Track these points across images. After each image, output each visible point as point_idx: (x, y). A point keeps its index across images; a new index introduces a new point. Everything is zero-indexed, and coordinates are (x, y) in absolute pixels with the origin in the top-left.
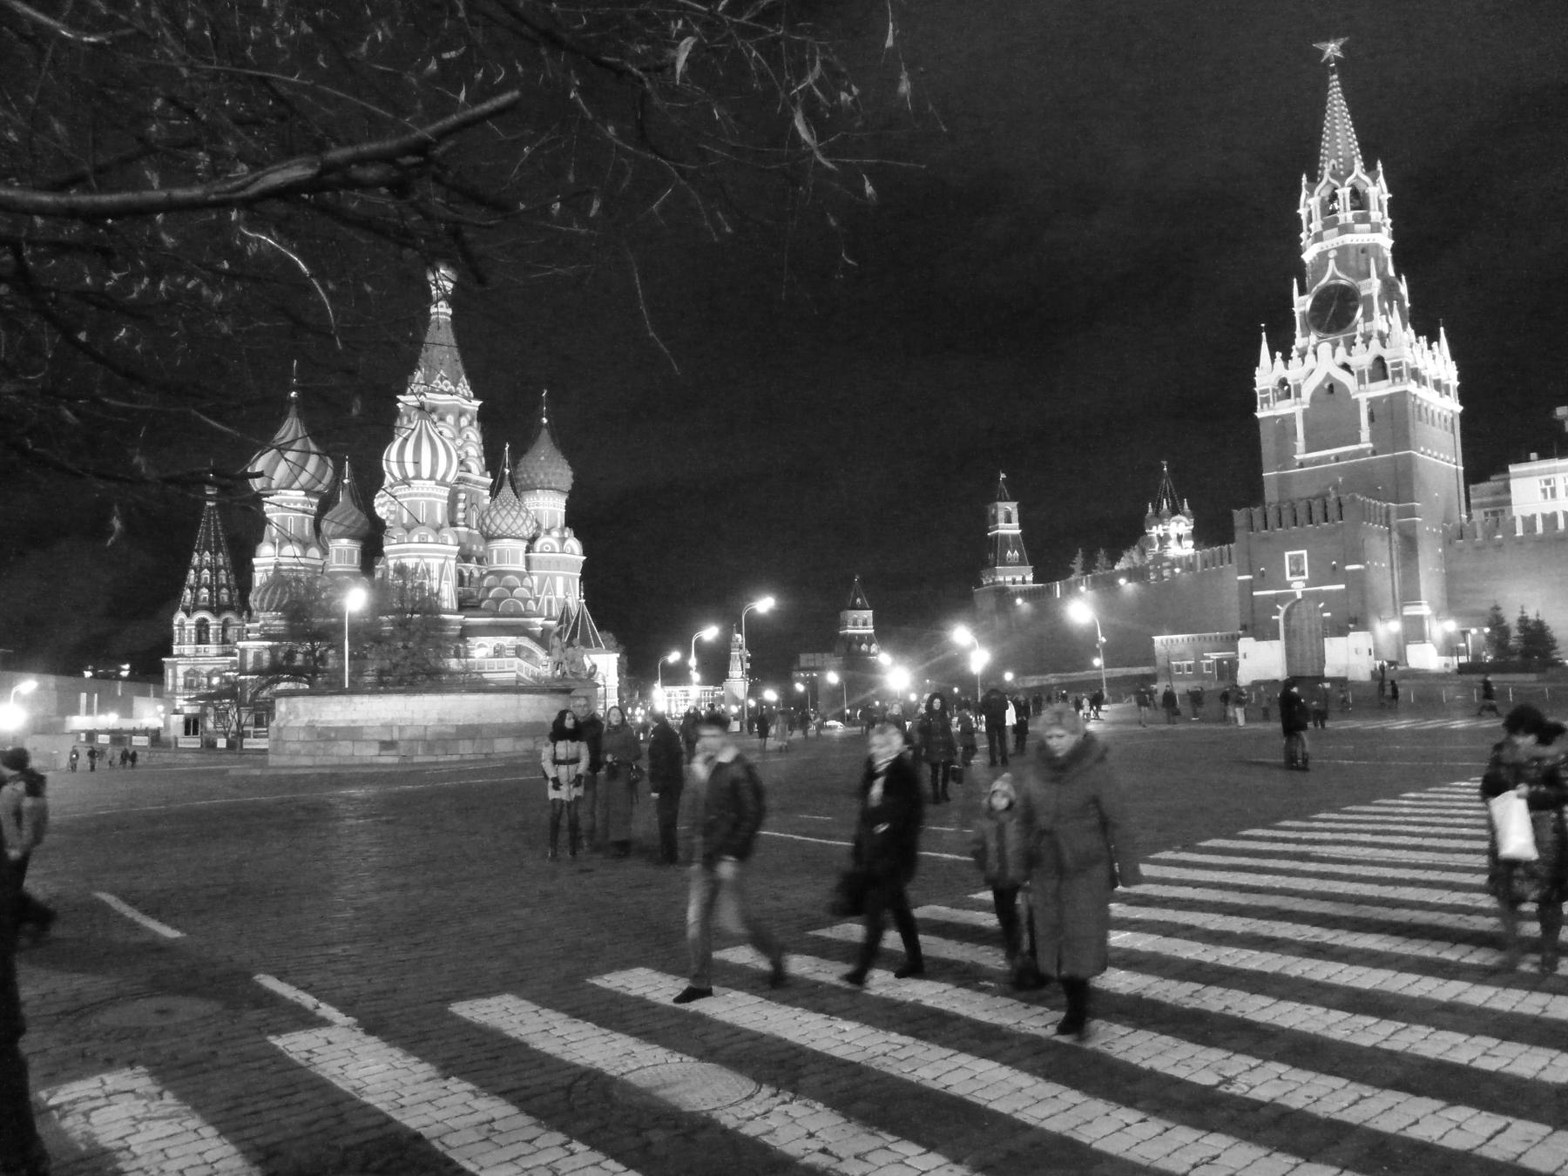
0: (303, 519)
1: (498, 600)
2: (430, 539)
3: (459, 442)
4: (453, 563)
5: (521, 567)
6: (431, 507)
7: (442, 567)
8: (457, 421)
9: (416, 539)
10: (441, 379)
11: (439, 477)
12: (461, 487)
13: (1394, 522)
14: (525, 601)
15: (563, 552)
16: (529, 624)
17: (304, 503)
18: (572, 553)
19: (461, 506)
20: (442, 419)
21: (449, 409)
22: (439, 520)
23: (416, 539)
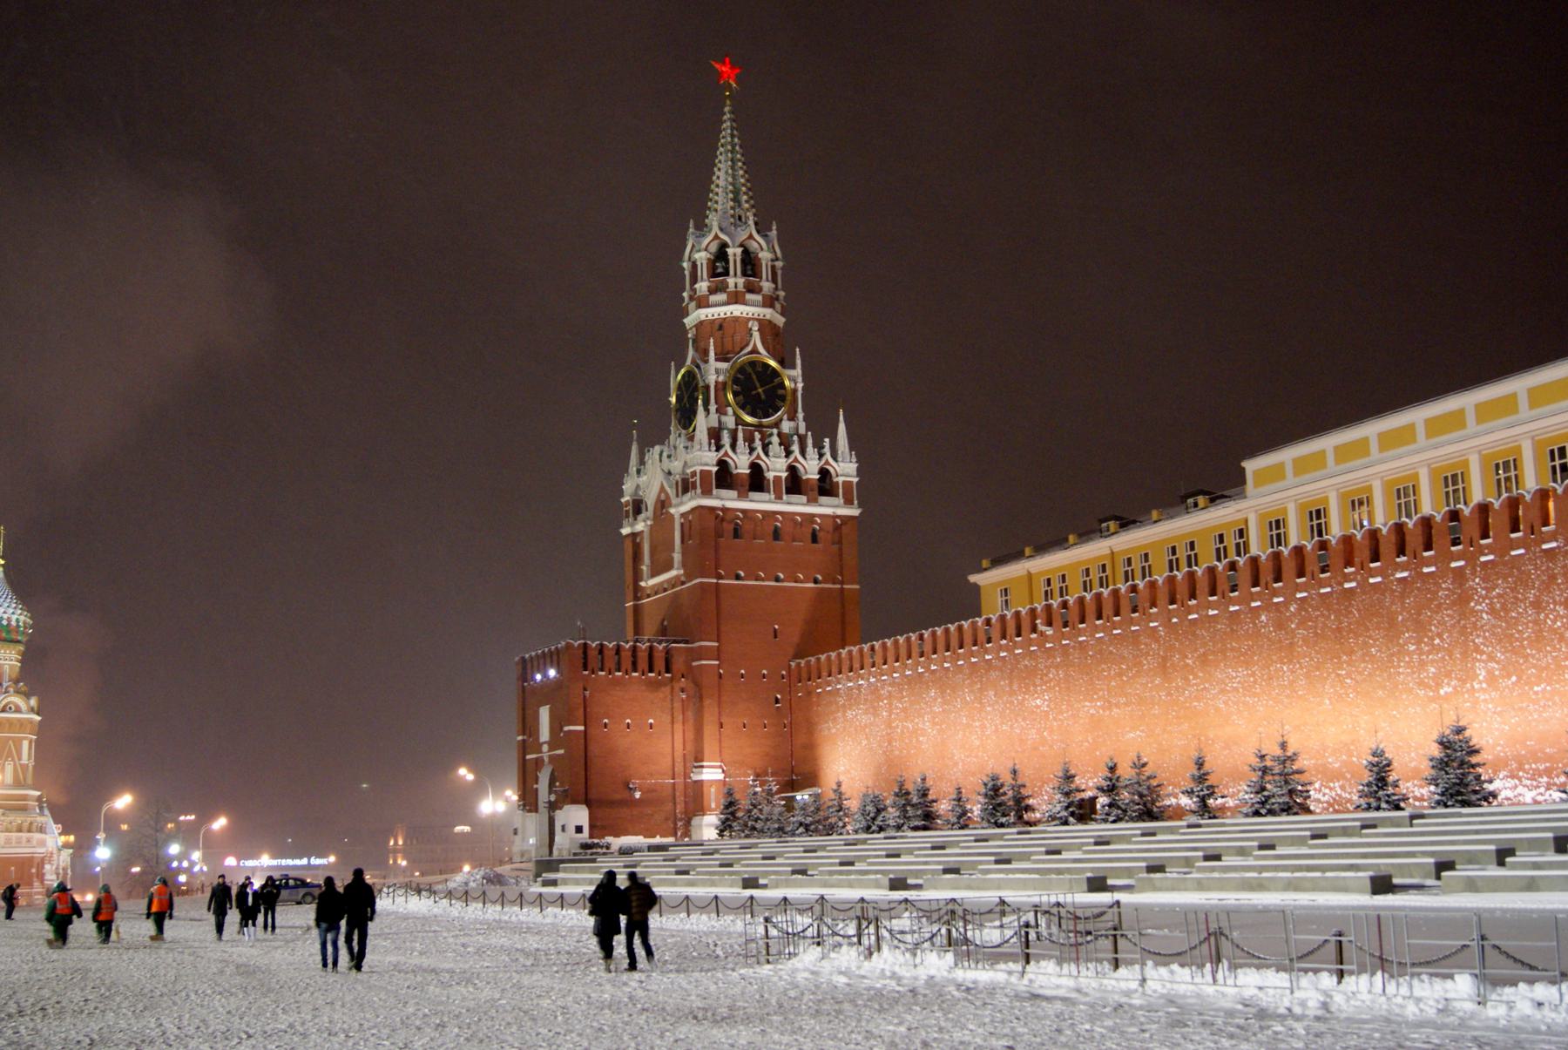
13: (678, 663)
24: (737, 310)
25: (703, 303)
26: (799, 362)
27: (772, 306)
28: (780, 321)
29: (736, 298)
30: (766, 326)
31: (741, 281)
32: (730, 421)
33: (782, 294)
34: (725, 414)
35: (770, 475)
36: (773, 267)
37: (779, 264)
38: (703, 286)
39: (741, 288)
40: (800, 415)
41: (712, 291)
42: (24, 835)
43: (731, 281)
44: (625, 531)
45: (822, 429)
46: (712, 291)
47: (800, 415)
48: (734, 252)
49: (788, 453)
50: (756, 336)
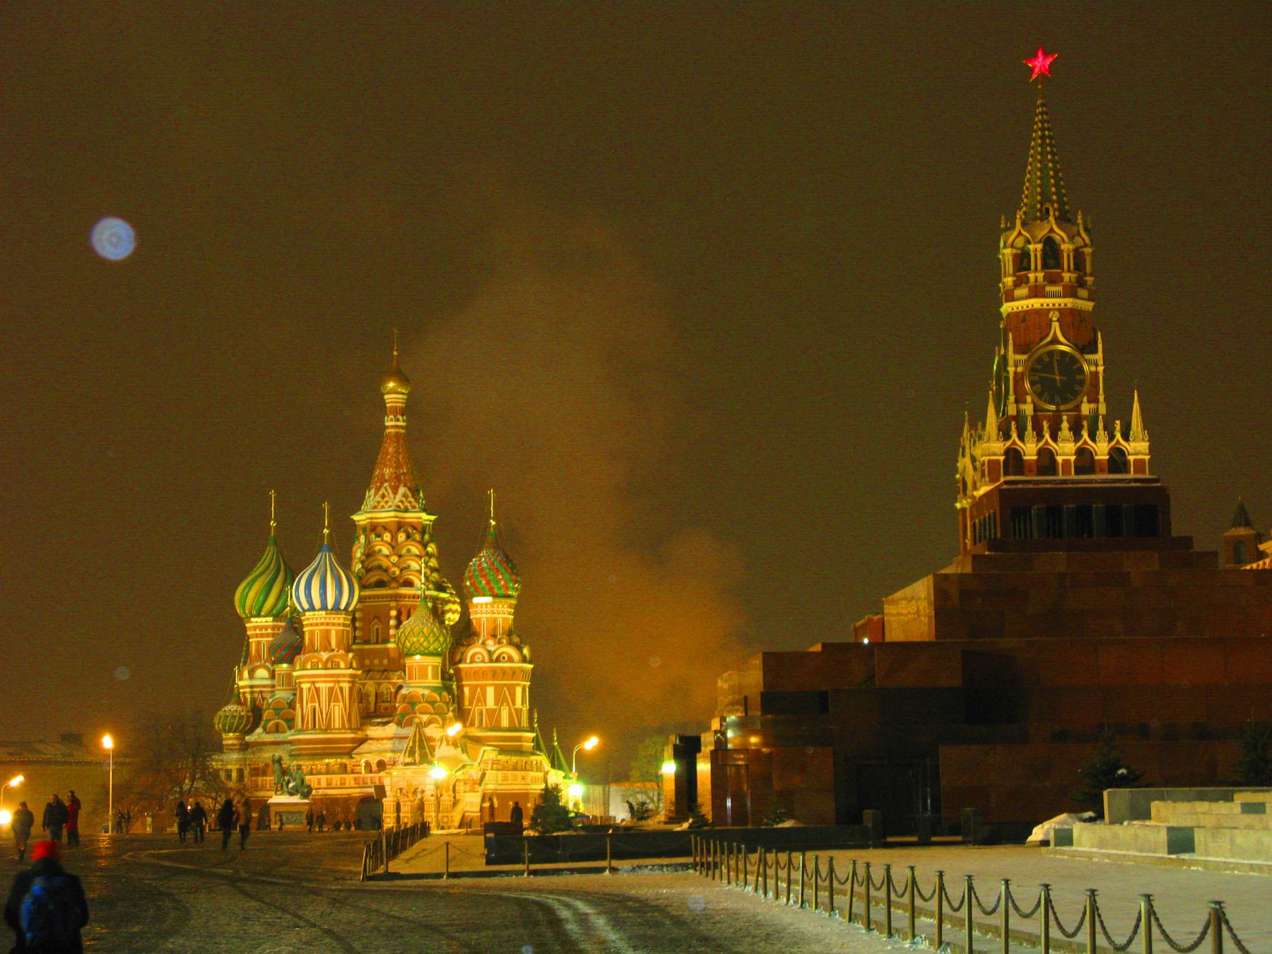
4: (346, 686)
6: (326, 634)
7: (331, 690)
8: (394, 537)
12: (393, 604)
17: (273, 628)
18: (511, 660)
19: (392, 622)
20: (379, 536)
23: (309, 666)
24: (1036, 303)
25: (1011, 298)
26: (1100, 346)
27: (1075, 295)
28: (1089, 306)
29: (1036, 292)
30: (1070, 319)
31: (1040, 275)
32: (1028, 409)
33: (1090, 280)
34: (1025, 402)
35: (1059, 459)
36: (1078, 254)
37: (1088, 250)
38: (1009, 281)
39: (1040, 279)
40: (1101, 398)
41: (1017, 284)
42: (510, 773)
43: (1031, 276)
44: (958, 505)
45: (1119, 411)
46: (1017, 284)
47: (1101, 398)
48: (1036, 248)
49: (1077, 436)
50: (1056, 325)
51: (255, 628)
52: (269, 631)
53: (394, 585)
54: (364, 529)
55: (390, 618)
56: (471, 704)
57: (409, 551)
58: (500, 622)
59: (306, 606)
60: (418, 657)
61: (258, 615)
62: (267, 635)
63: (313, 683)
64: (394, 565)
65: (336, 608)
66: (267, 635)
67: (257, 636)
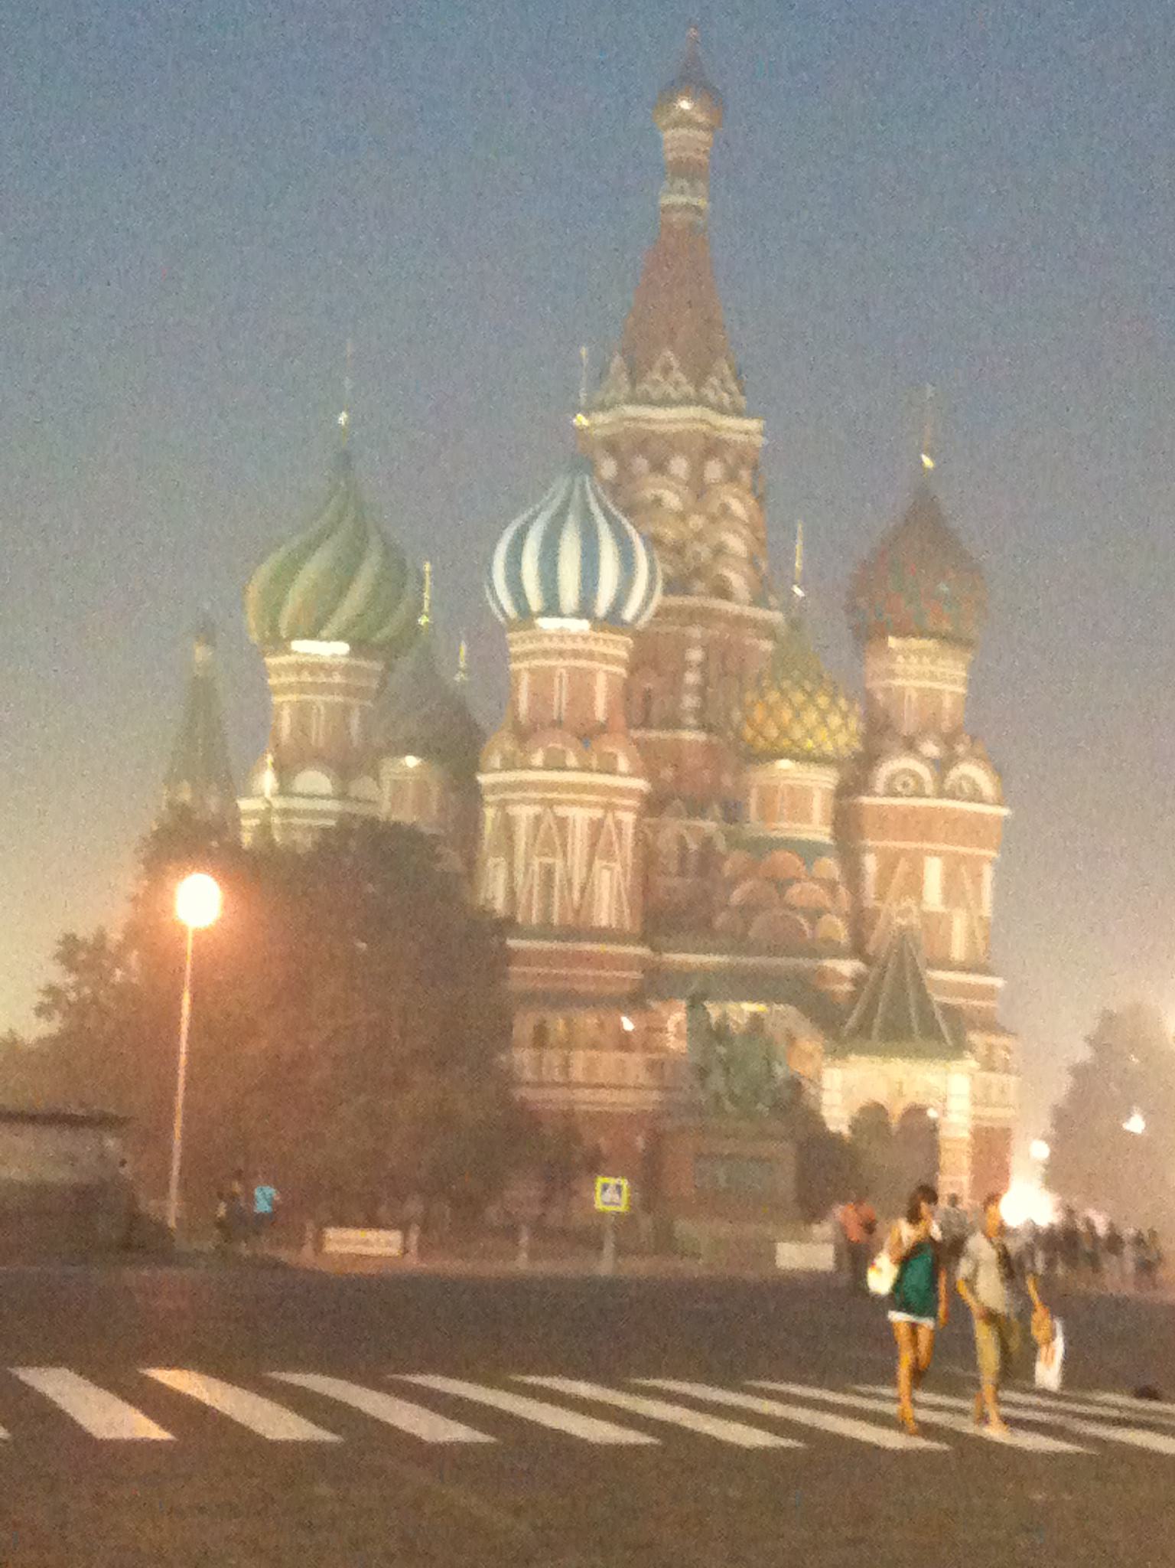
0: (346, 709)
1: (749, 910)
2: (572, 760)
3: (697, 521)
4: (628, 818)
5: (818, 830)
6: (581, 683)
7: (597, 827)
9: (538, 759)
10: (667, 370)
11: (602, 605)
12: (696, 632)
14: (816, 914)
15: (941, 794)
16: (822, 974)
17: (347, 670)
21: (674, 443)
22: (600, 712)
23: (538, 759)
51: (299, 668)
52: (337, 678)
53: (699, 586)
54: (612, 447)
55: (686, 666)
56: (881, 897)
57: (725, 509)
58: (947, 703)
59: (535, 602)
60: (784, 764)
61: (313, 634)
62: (329, 689)
63: (550, 804)
64: (699, 536)
65: (613, 621)
66: (329, 689)
67: (302, 688)
